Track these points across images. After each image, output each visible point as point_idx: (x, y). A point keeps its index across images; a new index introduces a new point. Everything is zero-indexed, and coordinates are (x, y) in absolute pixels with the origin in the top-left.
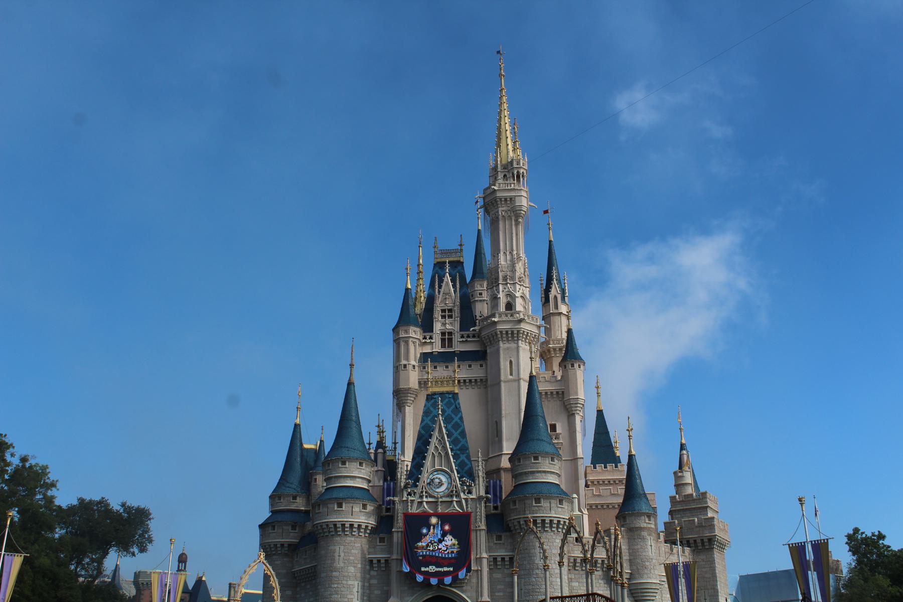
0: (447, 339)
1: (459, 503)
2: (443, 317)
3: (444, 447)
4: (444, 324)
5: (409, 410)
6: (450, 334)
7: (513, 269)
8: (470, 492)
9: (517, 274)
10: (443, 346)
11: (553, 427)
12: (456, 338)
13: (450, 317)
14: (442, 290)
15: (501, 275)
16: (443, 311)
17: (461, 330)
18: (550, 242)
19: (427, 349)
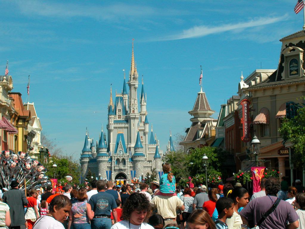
0: (119, 117)
1: (124, 156)
2: (119, 112)
3: (121, 146)
4: (119, 113)
5: (112, 133)
6: (120, 115)
7: (134, 102)
8: (126, 154)
9: (135, 103)
10: (119, 118)
11: (142, 137)
12: (122, 117)
13: (120, 112)
14: (118, 105)
15: (132, 103)
16: (119, 110)
17: (123, 115)
18: (143, 85)
19: (115, 119)
